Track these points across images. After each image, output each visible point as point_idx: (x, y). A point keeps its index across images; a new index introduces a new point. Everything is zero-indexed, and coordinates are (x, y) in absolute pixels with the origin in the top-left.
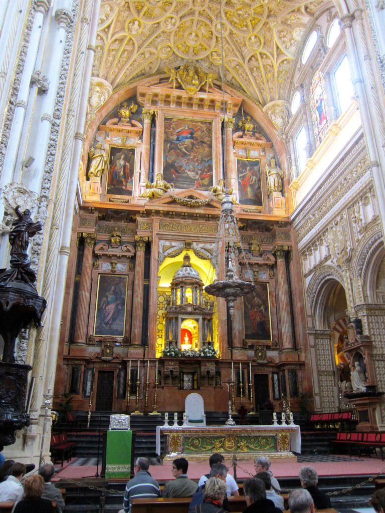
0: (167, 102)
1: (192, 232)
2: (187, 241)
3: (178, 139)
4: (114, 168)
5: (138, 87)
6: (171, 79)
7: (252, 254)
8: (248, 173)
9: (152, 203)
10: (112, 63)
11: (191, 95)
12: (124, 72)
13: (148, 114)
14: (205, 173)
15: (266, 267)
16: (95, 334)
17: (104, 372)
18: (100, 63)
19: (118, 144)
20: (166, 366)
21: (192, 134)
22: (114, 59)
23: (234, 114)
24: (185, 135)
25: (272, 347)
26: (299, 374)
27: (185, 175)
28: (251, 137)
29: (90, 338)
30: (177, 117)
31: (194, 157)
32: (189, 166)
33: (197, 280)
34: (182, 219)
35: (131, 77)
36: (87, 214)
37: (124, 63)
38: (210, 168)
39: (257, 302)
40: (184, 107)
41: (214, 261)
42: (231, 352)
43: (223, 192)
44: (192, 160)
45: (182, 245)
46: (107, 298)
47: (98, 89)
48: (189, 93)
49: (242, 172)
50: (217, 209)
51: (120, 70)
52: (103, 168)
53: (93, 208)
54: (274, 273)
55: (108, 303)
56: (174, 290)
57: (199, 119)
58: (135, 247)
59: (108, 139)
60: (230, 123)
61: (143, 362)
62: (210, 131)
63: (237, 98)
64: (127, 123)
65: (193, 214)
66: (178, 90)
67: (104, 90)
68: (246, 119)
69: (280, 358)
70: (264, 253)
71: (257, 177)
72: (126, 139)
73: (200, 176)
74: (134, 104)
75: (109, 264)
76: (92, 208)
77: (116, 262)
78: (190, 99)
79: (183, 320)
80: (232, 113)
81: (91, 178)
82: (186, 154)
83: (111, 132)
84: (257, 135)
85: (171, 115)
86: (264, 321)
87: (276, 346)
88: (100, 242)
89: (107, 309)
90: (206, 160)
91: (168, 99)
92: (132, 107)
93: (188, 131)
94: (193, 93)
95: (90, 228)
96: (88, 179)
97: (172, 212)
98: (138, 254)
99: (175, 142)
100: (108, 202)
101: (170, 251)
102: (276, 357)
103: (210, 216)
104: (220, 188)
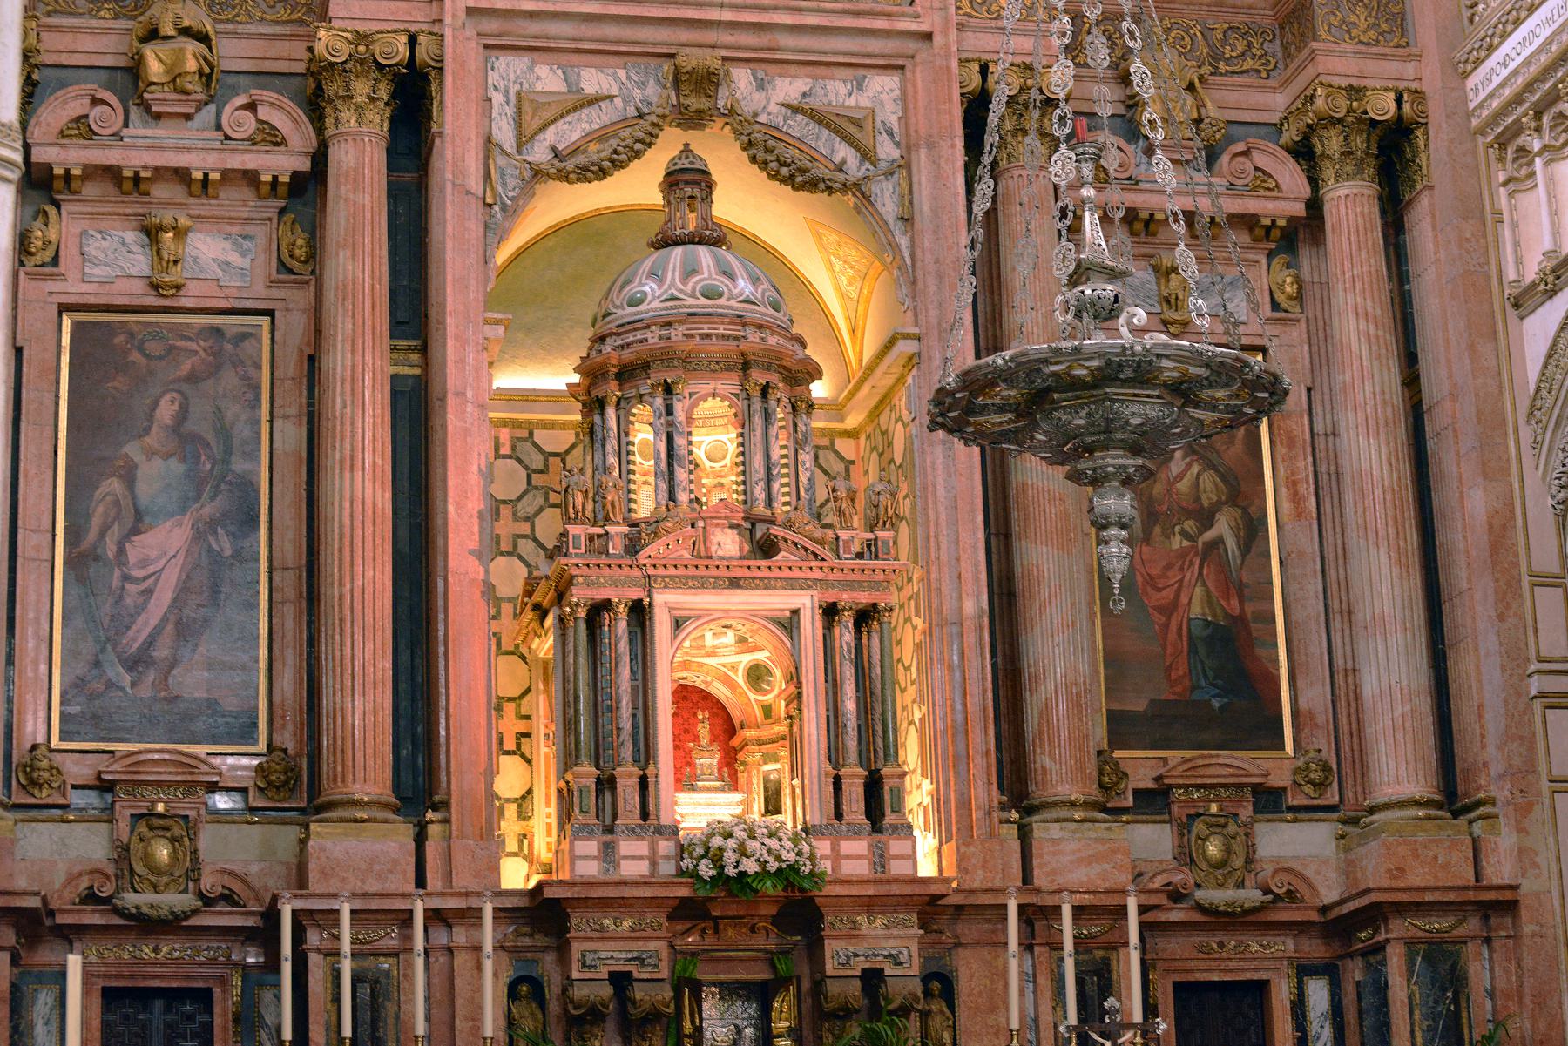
2: (692, 59)
15: (1245, 238)
16: (64, 736)
17: (144, 996)
20: (576, 948)
25: (1293, 800)
26: (1480, 970)
29: (29, 768)
33: (773, 340)
39: (1183, 486)
41: (886, 198)
45: (652, 91)
46: (129, 476)
54: (1298, 280)
55: (139, 515)
56: (611, 413)
58: (316, 107)
69: (1349, 869)
70: (1230, 140)
75: (132, 236)
77: (183, 221)
86: (1240, 620)
87: (1321, 786)
88: (62, 85)
89: (132, 560)
98: (342, 157)
102: (1326, 862)
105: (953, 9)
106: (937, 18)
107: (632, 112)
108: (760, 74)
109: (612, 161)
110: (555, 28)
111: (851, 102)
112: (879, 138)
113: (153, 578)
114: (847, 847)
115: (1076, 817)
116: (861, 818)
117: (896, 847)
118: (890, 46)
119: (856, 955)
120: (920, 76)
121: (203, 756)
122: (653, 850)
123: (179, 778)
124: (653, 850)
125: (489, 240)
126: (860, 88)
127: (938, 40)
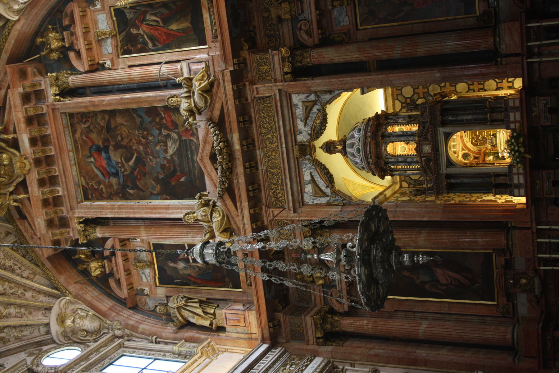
0: (57, 201)
1: (278, 148)
3: (116, 175)
4: (195, 278)
5: (46, 256)
6: (15, 204)
7: (300, 14)
8: (143, 30)
9: (239, 228)
10: (20, 306)
11: (30, 164)
12: (28, 282)
13: (87, 233)
14: (164, 121)
16: (495, 301)
18: (26, 325)
19: (152, 274)
21: (99, 150)
22: (11, 304)
23: (41, 74)
24: (104, 163)
27: (176, 159)
28: (72, 34)
30: (77, 180)
31: (139, 142)
32: (157, 152)
33: (369, 134)
34: (257, 169)
35: (33, 266)
36: (283, 330)
37: (13, 285)
38: (152, 111)
40: (57, 170)
42: (507, 56)
43: (190, 97)
44: (146, 146)
47: (69, 322)
48: (28, 167)
49: (145, 44)
50: (225, 107)
51: (27, 288)
52: (197, 305)
53: (271, 325)
57: (68, 142)
59: (147, 290)
60: (60, 82)
61: (541, 233)
62: (85, 116)
63: (9, 77)
64: (110, 261)
65: (243, 152)
66: (30, 189)
67: (68, 311)
68: (43, 43)
71: (145, 13)
72: (139, 262)
73: (170, 130)
74: (75, 252)
76: (270, 327)
78: (38, 162)
79: (450, 163)
80: (39, 78)
81: (221, 325)
82: (140, 161)
83: (135, 288)
84: (66, 22)
85: (76, 190)
89: (446, 283)
90: (138, 120)
91: (51, 200)
92: (83, 256)
93: (96, 156)
94: (26, 161)
95: (306, 325)
96: (221, 329)
97: (248, 191)
99: (121, 180)
100: (253, 287)
101: (322, 184)
103: (241, 118)
104: (184, 105)
105: (271, 84)
106: (274, 88)
107: (313, 167)
108: (298, 133)
109: (327, 175)
110: (295, 189)
111: (301, 108)
112: (310, 100)
113: (451, 278)
114: (512, 119)
115: (498, 40)
116: (503, 114)
117: (511, 104)
118: (284, 99)
119: (545, 116)
120: (290, 90)
121: (497, 271)
122: (515, 174)
123: (503, 278)
124: (515, 174)
125: (353, 204)
126: (297, 105)
127: (280, 87)
